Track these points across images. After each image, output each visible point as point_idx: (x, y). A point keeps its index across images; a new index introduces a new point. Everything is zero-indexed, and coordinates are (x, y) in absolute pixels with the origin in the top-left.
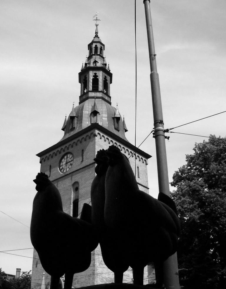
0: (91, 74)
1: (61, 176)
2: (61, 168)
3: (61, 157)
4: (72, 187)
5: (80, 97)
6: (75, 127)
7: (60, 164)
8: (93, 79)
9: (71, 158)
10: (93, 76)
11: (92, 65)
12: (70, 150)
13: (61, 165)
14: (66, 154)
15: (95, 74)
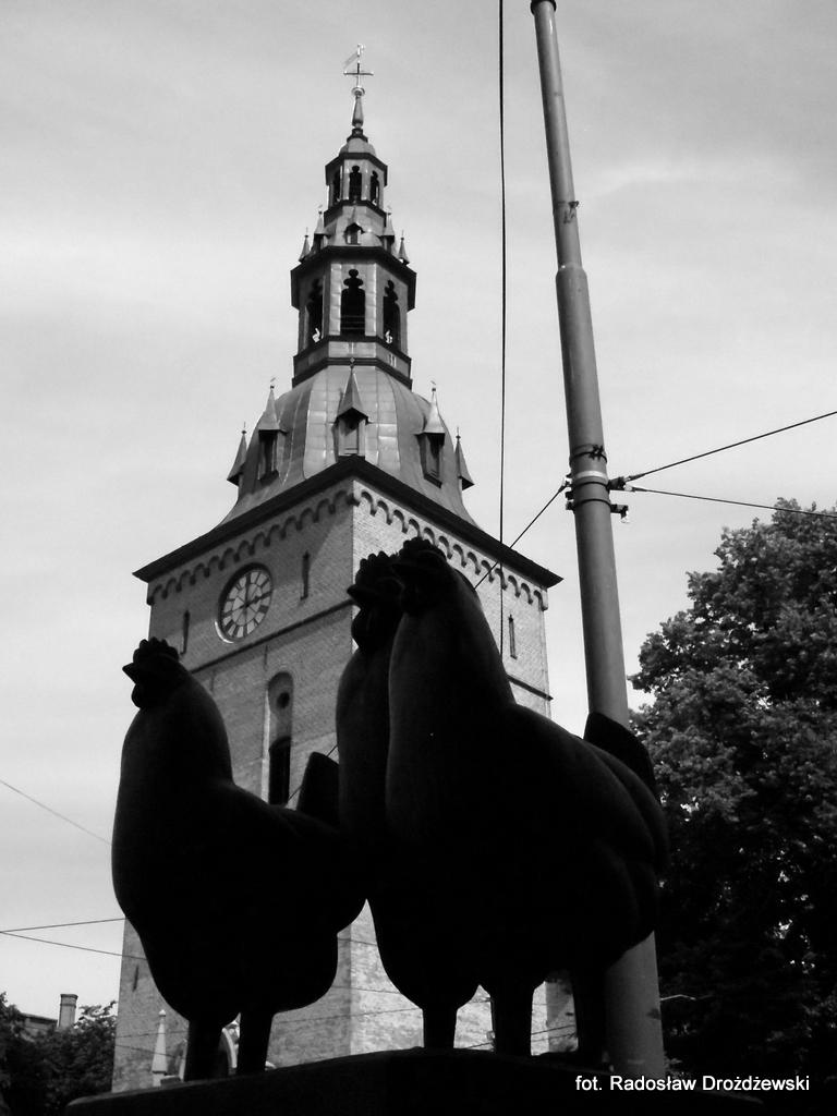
0: (338, 274)
1: (226, 652)
2: (226, 621)
3: (226, 580)
4: (267, 692)
5: (297, 359)
6: (276, 472)
7: (222, 606)
8: (344, 293)
9: (262, 587)
10: (346, 282)
11: (340, 241)
12: (261, 554)
13: (226, 610)
14: (246, 570)
15: (353, 273)
